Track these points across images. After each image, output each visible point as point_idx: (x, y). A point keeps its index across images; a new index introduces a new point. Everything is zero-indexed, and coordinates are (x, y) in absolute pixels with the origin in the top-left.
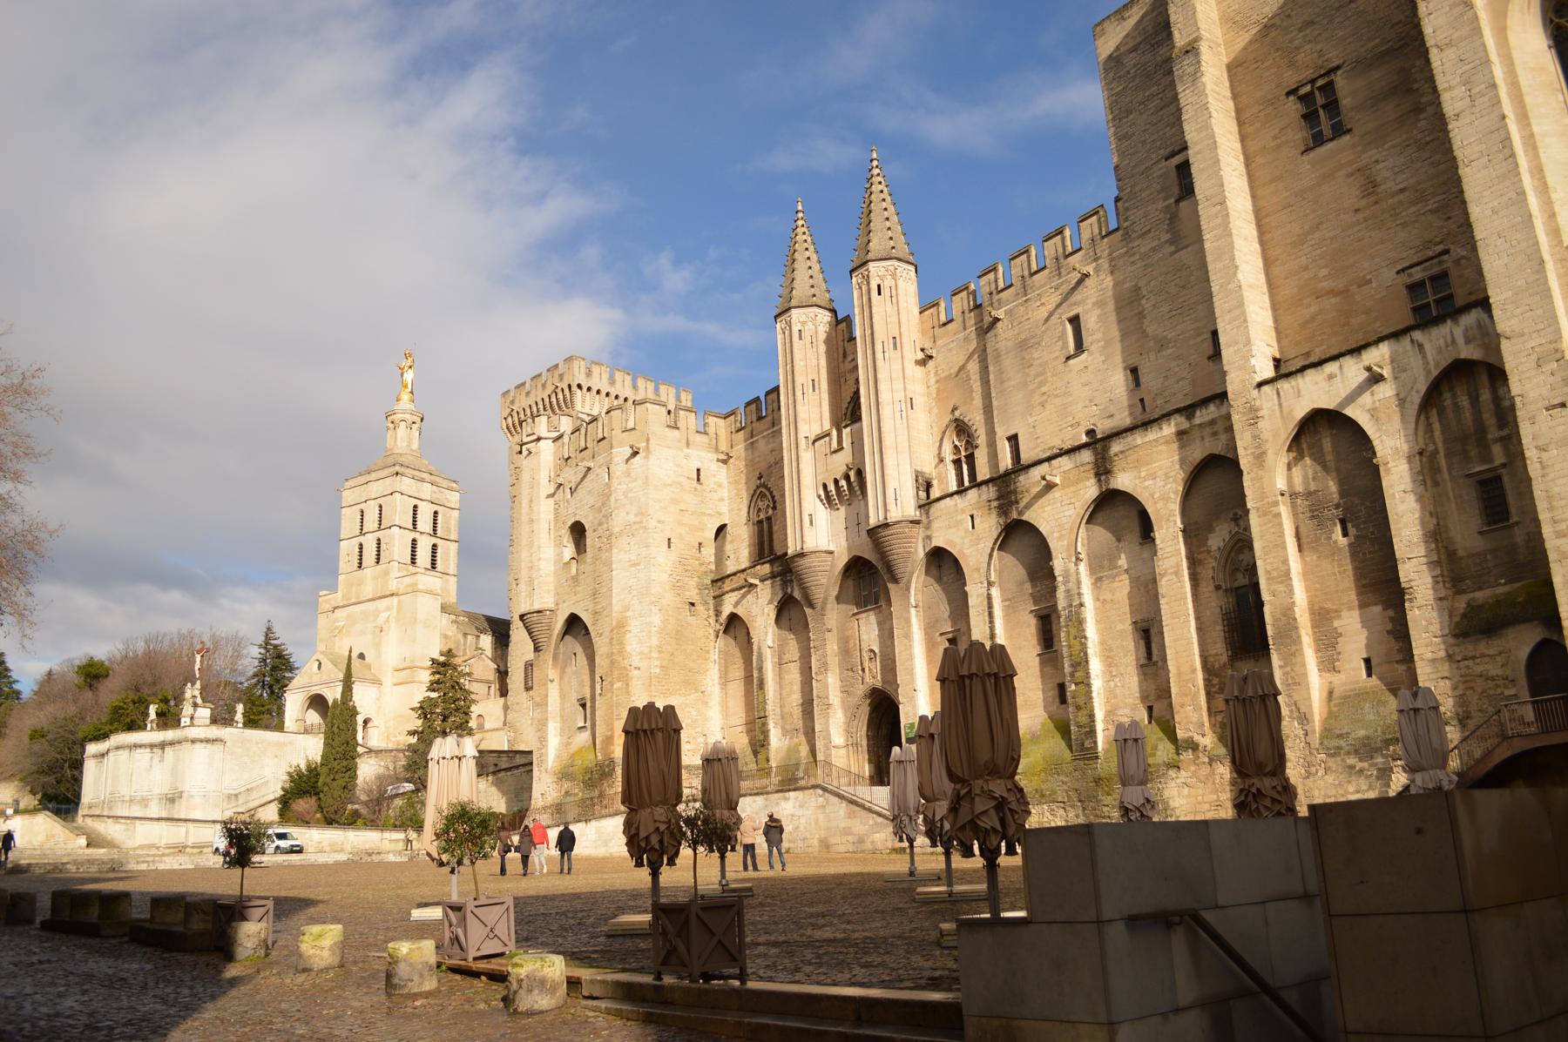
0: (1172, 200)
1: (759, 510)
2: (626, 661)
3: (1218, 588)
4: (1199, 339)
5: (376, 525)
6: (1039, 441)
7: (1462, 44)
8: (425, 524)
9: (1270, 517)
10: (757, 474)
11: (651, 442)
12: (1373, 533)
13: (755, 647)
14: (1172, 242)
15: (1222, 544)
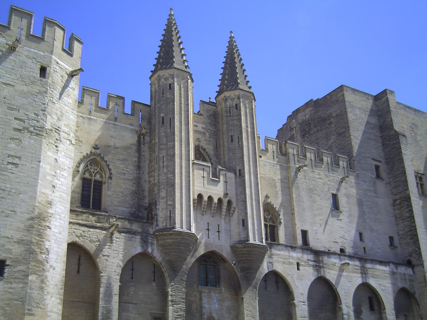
2: (44, 256)
6: (319, 241)
13: (104, 281)
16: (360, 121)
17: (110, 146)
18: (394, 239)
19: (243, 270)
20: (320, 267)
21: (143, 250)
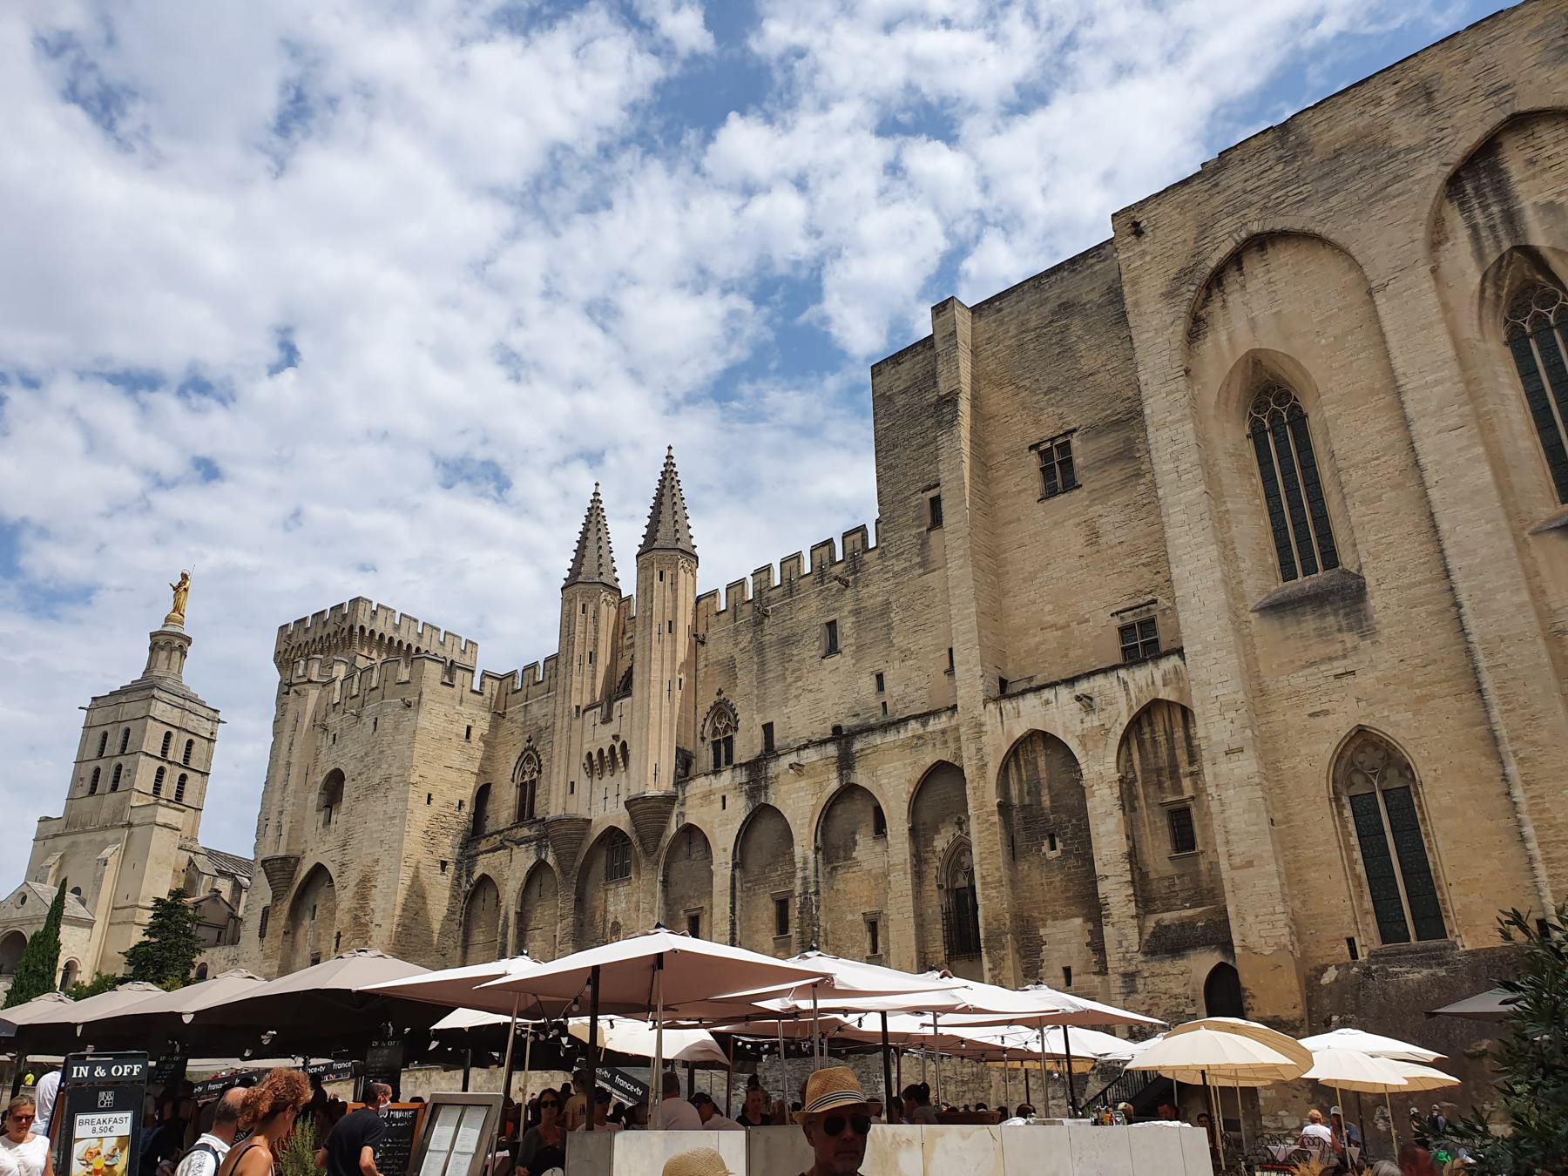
0: (925, 528)
1: (524, 772)
2: (367, 918)
3: (940, 887)
4: (939, 654)
5: (117, 750)
7: (1172, 427)
8: (175, 753)
9: (987, 825)
11: (424, 696)
12: (1077, 849)
13: (503, 912)
14: (922, 565)
15: (946, 846)
16: (905, 419)
19: (642, 839)
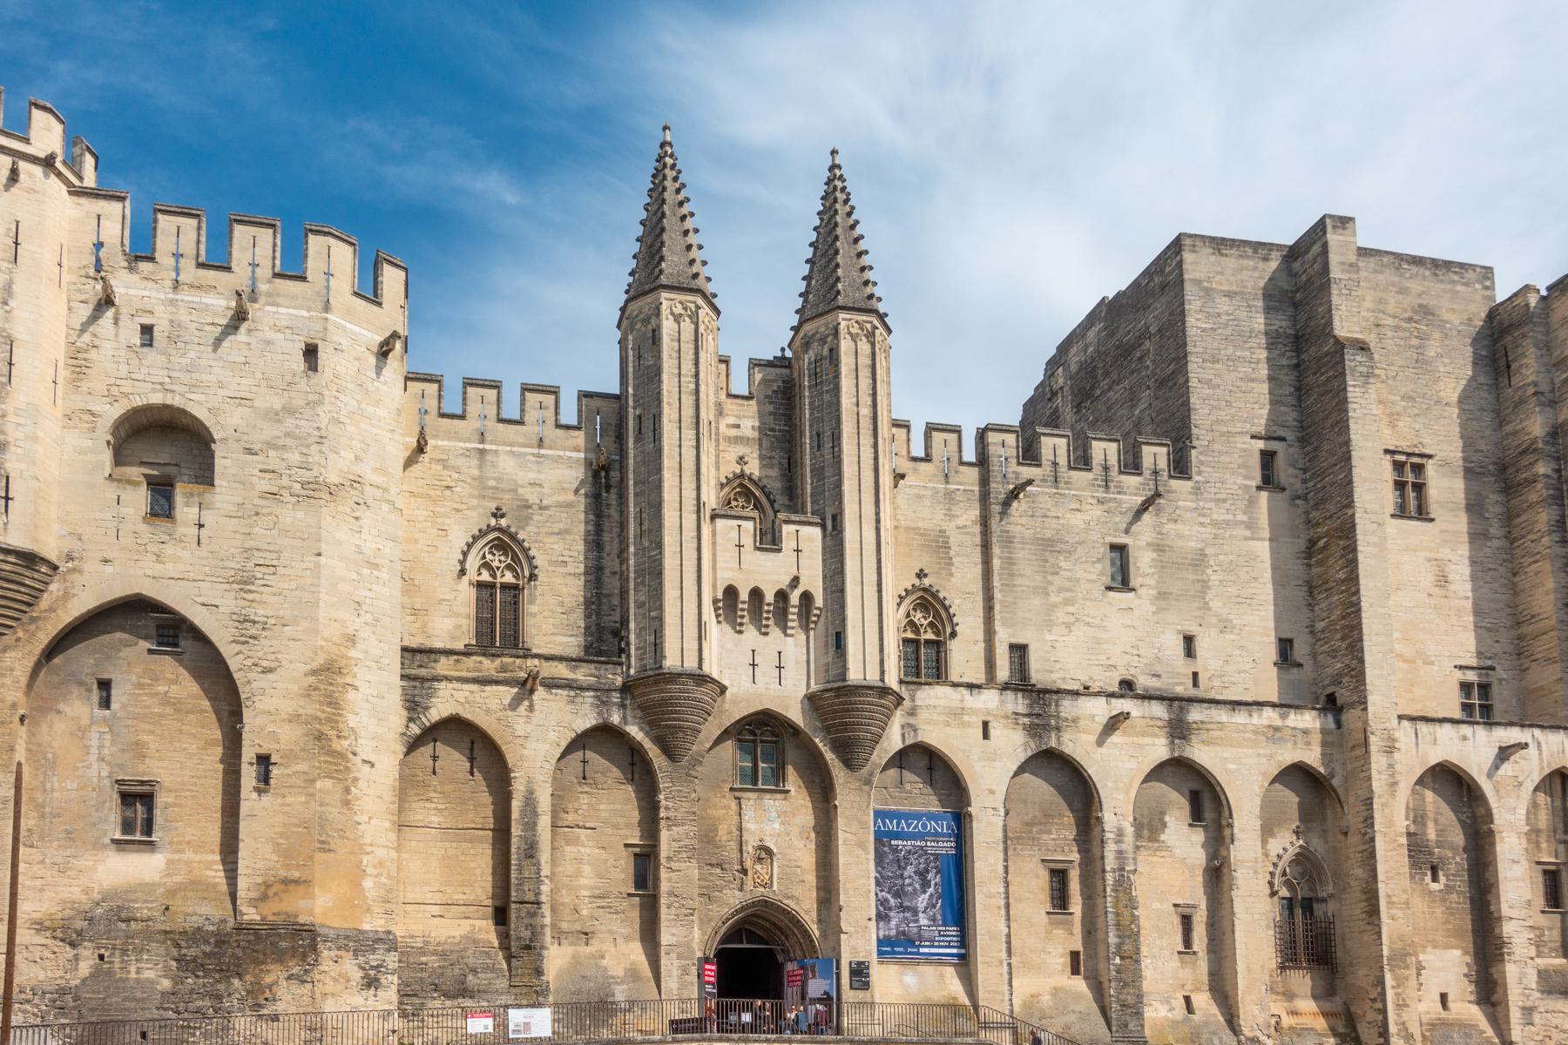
9: (1395, 845)
10: (492, 506)
17: (529, 507)
18: (1296, 645)
20: (1046, 727)
21: (601, 721)
